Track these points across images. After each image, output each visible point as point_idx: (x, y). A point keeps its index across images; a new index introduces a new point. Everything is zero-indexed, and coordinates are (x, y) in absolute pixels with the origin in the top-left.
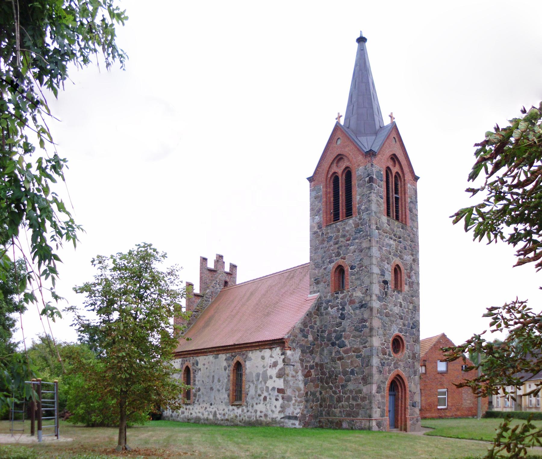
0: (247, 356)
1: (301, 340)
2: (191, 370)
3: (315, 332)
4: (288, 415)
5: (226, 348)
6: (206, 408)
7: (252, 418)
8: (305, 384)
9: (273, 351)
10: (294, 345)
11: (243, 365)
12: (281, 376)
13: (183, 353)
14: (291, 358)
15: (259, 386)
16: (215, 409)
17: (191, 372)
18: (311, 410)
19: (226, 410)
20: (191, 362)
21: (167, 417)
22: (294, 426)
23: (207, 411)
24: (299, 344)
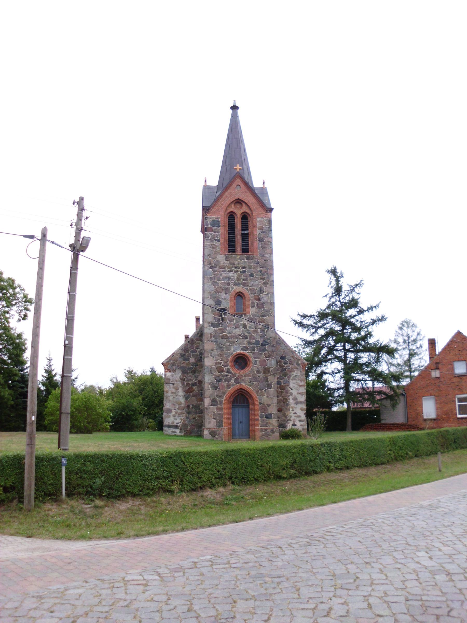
3: (197, 355)
8: (186, 399)
10: (174, 367)
14: (171, 378)
18: (192, 420)
22: (174, 434)
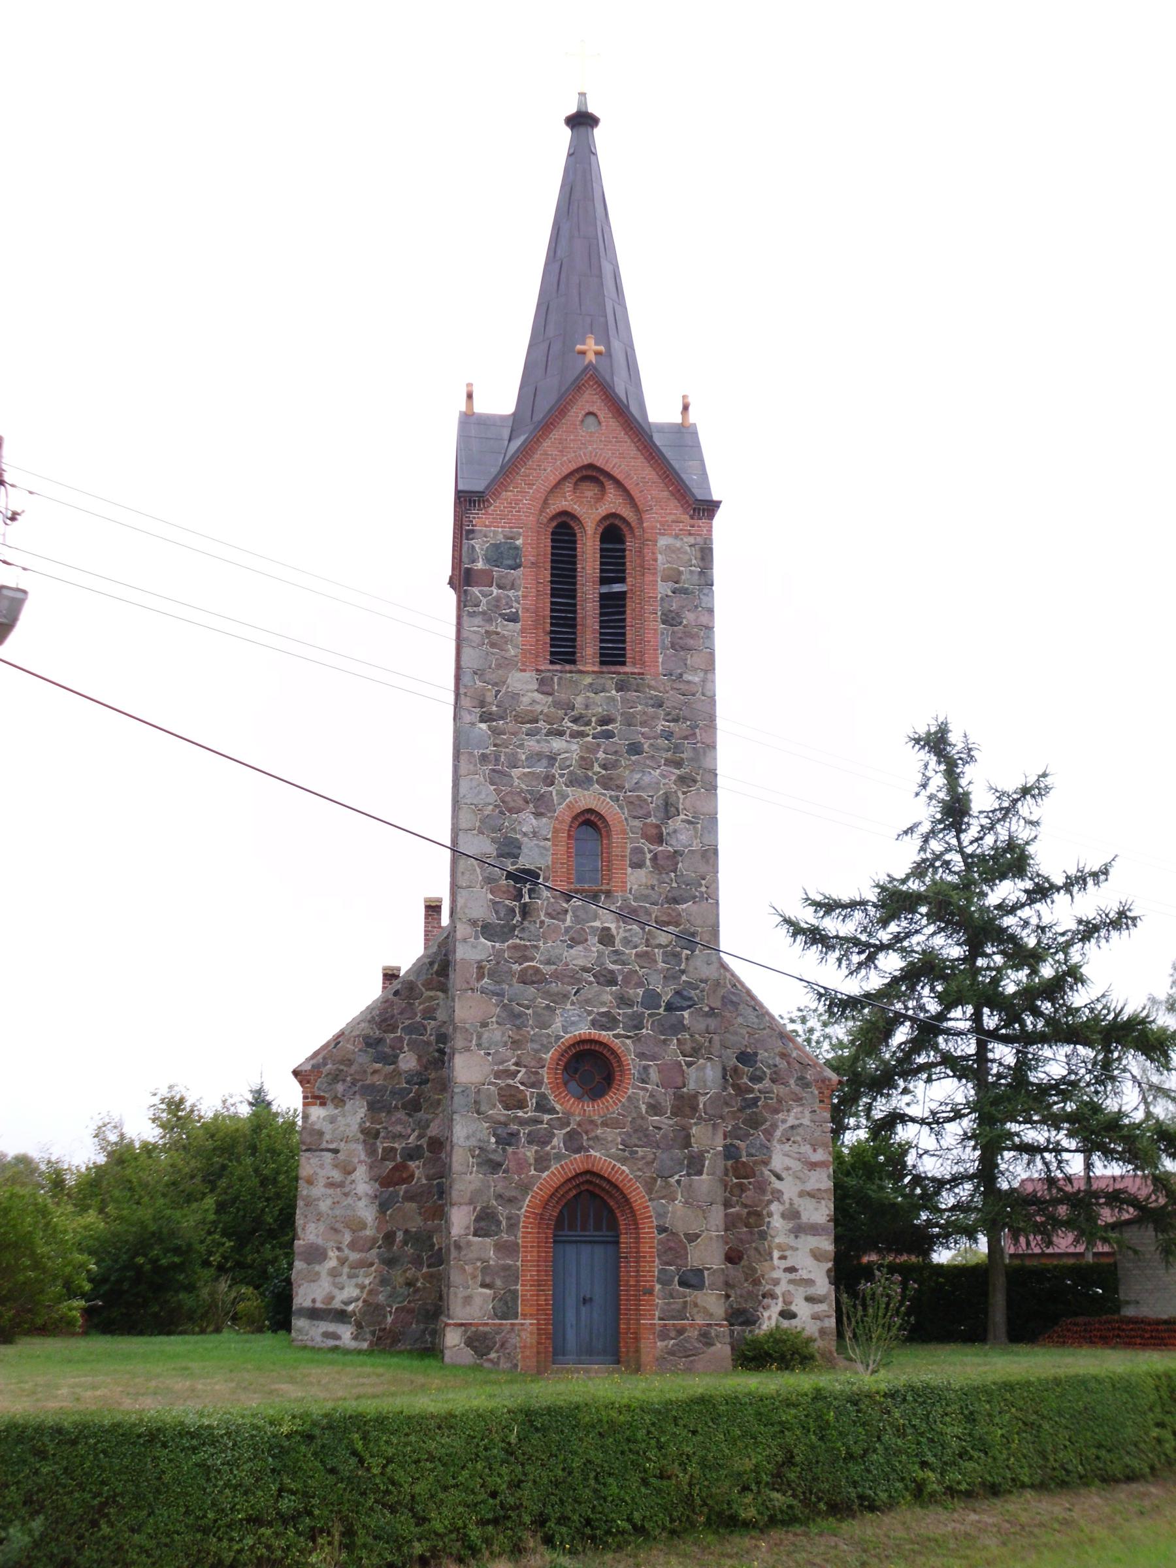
10: (340, 1087)
14: (327, 1128)
22: (332, 1343)
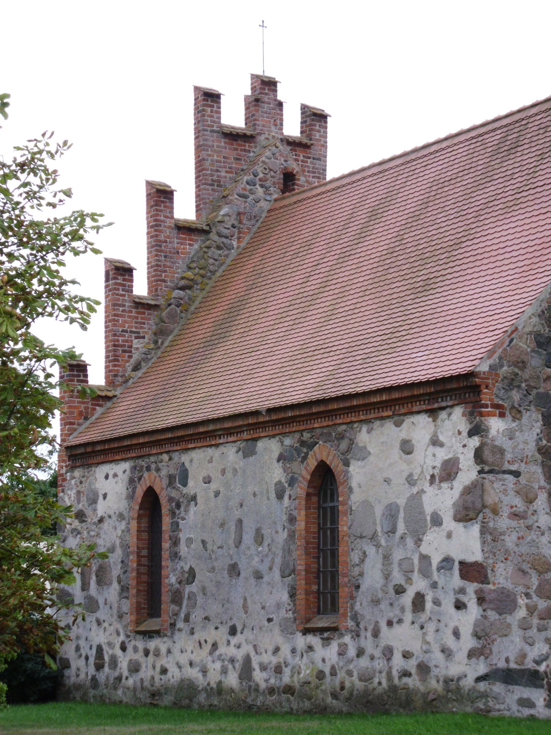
0: (352, 442)
1: (543, 376)
2: (163, 501)
4: (502, 664)
5: (282, 415)
6: (215, 646)
7: (376, 680)
9: (439, 420)
10: (516, 396)
11: (340, 478)
12: (472, 514)
13: (135, 441)
14: (507, 445)
15: (398, 555)
16: (247, 649)
17: (165, 510)
19: (286, 650)
20: (164, 472)
21: (78, 687)
22: (527, 712)
23: (220, 657)
24: (535, 392)
